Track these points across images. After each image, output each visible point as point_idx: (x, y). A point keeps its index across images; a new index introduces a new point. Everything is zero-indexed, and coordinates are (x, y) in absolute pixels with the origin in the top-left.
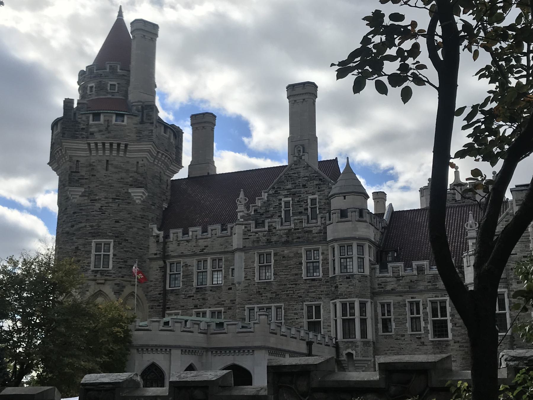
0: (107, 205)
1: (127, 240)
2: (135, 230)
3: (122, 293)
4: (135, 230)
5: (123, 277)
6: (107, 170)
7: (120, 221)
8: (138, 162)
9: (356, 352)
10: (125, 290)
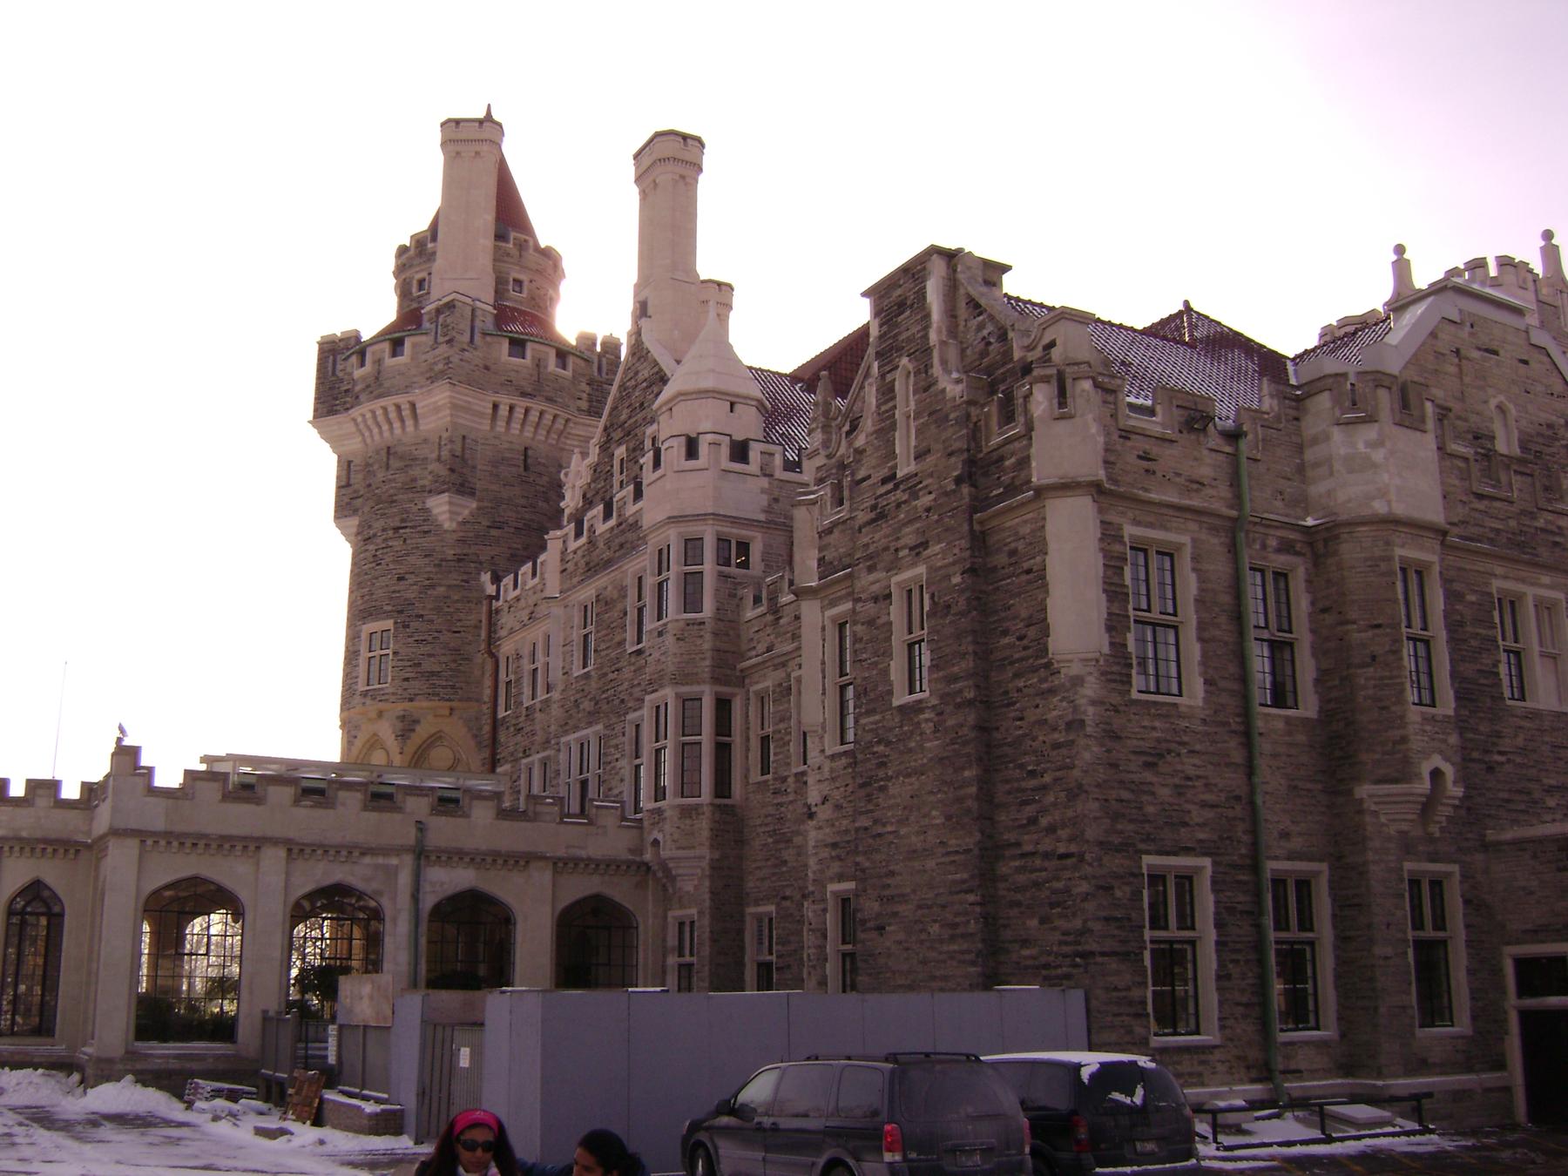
0: (384, 545)
1: (422, 616)
2: (441, 590)
3: (412, 734)
4: (441, 590)
5: (411, 700)
6: (388, 467)
7: (407, 576)
8: (440, 437)
10: (418, 728)
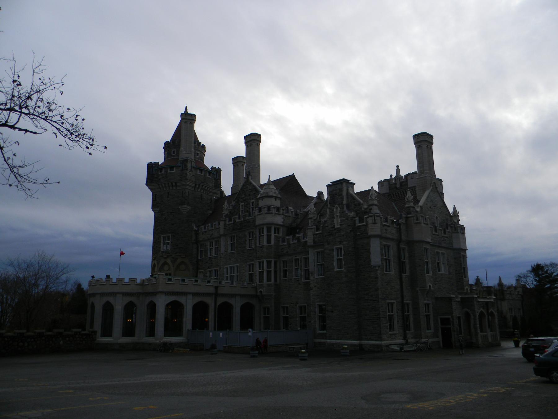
6: (168, 197)
9: (264, 291)
